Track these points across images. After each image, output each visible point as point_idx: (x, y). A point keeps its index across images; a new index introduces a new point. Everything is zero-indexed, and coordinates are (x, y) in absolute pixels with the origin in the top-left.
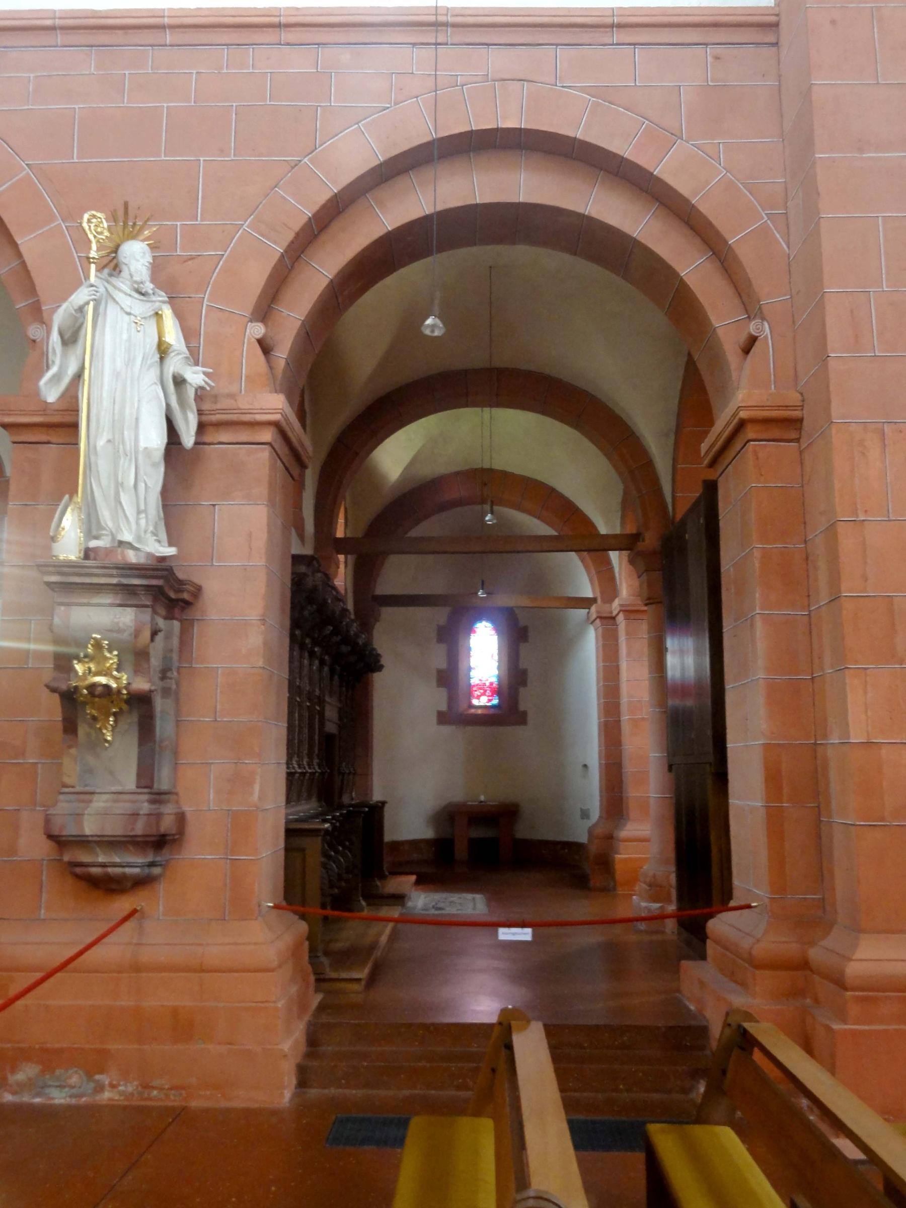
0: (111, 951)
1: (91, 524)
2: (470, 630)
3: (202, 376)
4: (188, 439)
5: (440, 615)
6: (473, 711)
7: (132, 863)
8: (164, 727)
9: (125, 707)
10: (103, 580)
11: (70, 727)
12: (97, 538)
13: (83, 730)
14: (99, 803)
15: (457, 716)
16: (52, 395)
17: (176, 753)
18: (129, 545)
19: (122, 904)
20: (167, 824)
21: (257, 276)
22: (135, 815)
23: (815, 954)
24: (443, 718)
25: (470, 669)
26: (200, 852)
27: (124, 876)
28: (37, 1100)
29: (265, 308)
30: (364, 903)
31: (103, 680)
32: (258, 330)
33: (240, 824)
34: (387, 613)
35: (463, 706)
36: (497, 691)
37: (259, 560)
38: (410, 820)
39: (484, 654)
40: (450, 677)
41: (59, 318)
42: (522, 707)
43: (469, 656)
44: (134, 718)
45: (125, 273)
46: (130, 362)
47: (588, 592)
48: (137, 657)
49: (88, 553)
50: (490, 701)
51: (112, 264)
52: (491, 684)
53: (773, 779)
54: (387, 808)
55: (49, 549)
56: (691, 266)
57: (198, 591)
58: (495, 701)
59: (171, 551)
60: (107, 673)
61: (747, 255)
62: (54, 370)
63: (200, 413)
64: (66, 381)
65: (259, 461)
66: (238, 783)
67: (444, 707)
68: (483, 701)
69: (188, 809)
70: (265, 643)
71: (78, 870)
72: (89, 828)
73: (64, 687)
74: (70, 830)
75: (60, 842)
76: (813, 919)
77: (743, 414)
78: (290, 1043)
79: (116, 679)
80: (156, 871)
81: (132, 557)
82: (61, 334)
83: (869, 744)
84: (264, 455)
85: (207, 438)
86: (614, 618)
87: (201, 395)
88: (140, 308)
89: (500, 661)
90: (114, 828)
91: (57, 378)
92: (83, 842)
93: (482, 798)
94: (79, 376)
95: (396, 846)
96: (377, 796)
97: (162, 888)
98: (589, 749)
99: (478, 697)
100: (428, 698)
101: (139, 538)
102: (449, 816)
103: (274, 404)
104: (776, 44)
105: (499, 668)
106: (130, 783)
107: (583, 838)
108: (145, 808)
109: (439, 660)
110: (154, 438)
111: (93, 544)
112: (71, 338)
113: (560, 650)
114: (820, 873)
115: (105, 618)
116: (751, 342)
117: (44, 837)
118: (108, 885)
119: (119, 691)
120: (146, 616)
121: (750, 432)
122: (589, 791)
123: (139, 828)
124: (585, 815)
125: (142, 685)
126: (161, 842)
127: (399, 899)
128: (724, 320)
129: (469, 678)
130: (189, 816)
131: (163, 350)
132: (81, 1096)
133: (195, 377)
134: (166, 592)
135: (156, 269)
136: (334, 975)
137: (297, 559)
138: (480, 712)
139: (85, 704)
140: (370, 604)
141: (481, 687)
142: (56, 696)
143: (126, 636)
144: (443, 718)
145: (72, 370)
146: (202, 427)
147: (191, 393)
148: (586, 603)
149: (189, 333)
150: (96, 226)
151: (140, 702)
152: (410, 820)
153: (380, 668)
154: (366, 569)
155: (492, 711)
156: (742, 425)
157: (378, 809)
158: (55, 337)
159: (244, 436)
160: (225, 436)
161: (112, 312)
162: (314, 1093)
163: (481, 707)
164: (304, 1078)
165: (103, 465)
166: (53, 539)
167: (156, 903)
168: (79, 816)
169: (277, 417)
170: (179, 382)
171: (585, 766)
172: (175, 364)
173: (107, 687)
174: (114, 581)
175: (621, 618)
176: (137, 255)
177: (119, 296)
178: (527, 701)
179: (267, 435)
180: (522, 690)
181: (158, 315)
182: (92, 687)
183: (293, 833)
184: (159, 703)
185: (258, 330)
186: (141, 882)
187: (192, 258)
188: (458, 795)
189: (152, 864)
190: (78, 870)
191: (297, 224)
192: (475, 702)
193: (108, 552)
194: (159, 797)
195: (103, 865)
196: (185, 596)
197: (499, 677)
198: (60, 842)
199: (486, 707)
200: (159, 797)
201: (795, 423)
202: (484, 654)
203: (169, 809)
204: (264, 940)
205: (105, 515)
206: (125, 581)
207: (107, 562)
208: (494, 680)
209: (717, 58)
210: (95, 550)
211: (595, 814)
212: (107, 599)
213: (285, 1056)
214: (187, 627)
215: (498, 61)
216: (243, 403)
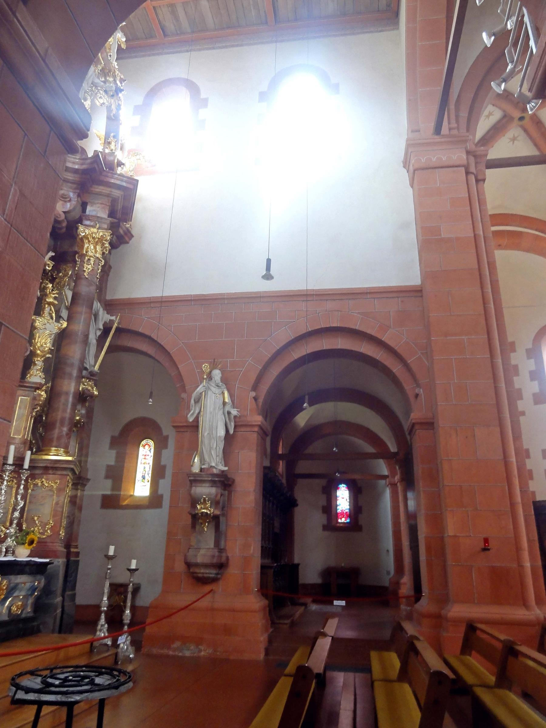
0: (205, 603)
1: (202, 460)
3: (236, 412)
4: (231, 431)
5: (323, 482)
6: (338, 525)
7: (211, 573)
8: (222, 527)
9: (211, 520)
10: (206, 479)
11: (194, 526)
12: (204, 464)
13: (198, 527)
14: (202, 552)
16: (191, 420)
17: (226, 537)
18: (214, 467)
19: (207, 588)
20: (223, 560)
21: (253, 377)
22: (213, 556)
23: (443, 612)
24: (326, 528)
25: (337, 506)
26: (233, 571)
27: (209, 578)
28: (180, 654)
29: (255, 388)
30: (289, 604)
31: (205, 511)
32: (253, 394)
33: (246, 560)
34: (300, 481)
35: (334, 523)
36: (349, 516)
37: (253, 470)
38: (310, 574)
39: (343, 499)
41: (194, 395)
42: (360, 523)
43: (336, 500)
44: (214, 523)
45: (213, 380)
46: (214, 409)
47: (386, 472)
48: (216, 503)
49: (201, 470)
50: (346, 520)
51: (210, 377)
52: (346, 513)
53: (429, 549)
54: (300, 567)
55: (190, 468)
56: (396, 369)
57: (234, 481)
58: (348, 520)
59: (226, 468)
60: (207, 509)
61: (414, 367)
62: (192, 412)
63: (235, 422)
64: (195, 415)
65: (253, 437)
66: (245, 546)
67: (325, 522)
68: (343, 520)
69: (230, 555)
70: (255, 499)
71: (195, 575)
72: (199, 560)
73: (194, 513)
74: (193, 561)
75: (189, 565)
76: (443, 600)
77: (413, 421)
78: (263, 638)
79: (210, 511)
80: (219, 576)
81: (215, 471)
82: (194, 400)
83: (455, 536)
84: (255, 435)
85: (237, 430)
86: (396, 484)
87: (235, 417)
88: (217, 391)
89: (350, 502)
90: (207, 560)
91: (193, 414)
92: (197, 565)
93: (343, 565)
94: (199, 413)
95: (305, 586)
96: (296, 561)
97: (221, 582)
98: (388, 543)
99: (341, 519)
100: (318, 519)
101: (217, 465)
102: (328, 573)
103: (258, 419)
104: (422, 296)
105: (350, 505)
106: (212, 545)
107: (387, 584)
108: (217, 554)
109: (323, 501)
110: (222, 433)
111: (203, 467)
112: (197, 401)
113: (377, 497)
114: (445, 584)
115: (205, 490)
116: (417, 396)
117: (183, 563)
118: (203, 581)
119: (210, 514)
120: (220, 491)
121: (417, 427)
122: (389, 562)
123: (215, 561)
124: (388, 573)
125: (217, 512)
126: (221, 566)
127: (305, 605)
128: (408, 386)
129: (337, 510)
130: (230, 558)
131: (224, 403)
132: (194, 653)
133: (234, 412)
134: (225, 482)
135: (223, 380)
136: (278, 622)
137: (265, 468)
138: (341, 525)
139: (199, 519)
140: (293, 477)
141: (342, 514)
142: (190, 516)
143: (213, 497)
144: (326, 528)
145: (197, 412)
146: (235, 427)
147: (232, 417)
148: (384, 477)
149: (231, 396)
150: (206, 367)
151: (216, 519)
152: (310, 574)
153: (297, 505)
154: (290, 466)
155: (347, 525)
156: (413, 425)
157: (296, 567)
158: (192, 401)
159: (248, 429)
160: (242, 429)
161: (210, 393)
162: (271, 657)
163: (342, 523)
164: (267, 652)
165: (206, 441)
166: (192, 466)
167: (219, 587)
168: (196, 556)
169: (260, 423)
170: (229, 413)
171: (388, 551)
172: (228, 408)
173: (207, 513)
174: (210, 479)
175: (398, 484)
176: (217, 374)
177: (212, 388)
178: (363, 520)
179: (256, 429)
180: (360, 515)
181: (223, 393)
182: (203, 512)
183: (263, 568)
184: (222, 519)
185: (253, 394)
186: (214, 580)
187: (232, 371)
188: (332, 563)
189: (217, 574)
190: (195, 575)
191: (267, 359)
192: (339, 521)
193: (208, 469)
194: (221, 551)
195: (203, 573)
196: (230, 483)
197: (350, 509)
198: (189, 565)
199: (344, 523)
200: (221, 551)
201: (433, 424)
202: (343, 499)
203: (224, 555)
204: (255, 602)
205: (206, 457)
206: (213, 479)
207: (209, 472)
208: (348, 511)
209: (402, 301)
210: (204, 468)
212: (207, 485)
213: (261, 642)
214: (230, 493)
215: (330, 305)
216: (249, 419)
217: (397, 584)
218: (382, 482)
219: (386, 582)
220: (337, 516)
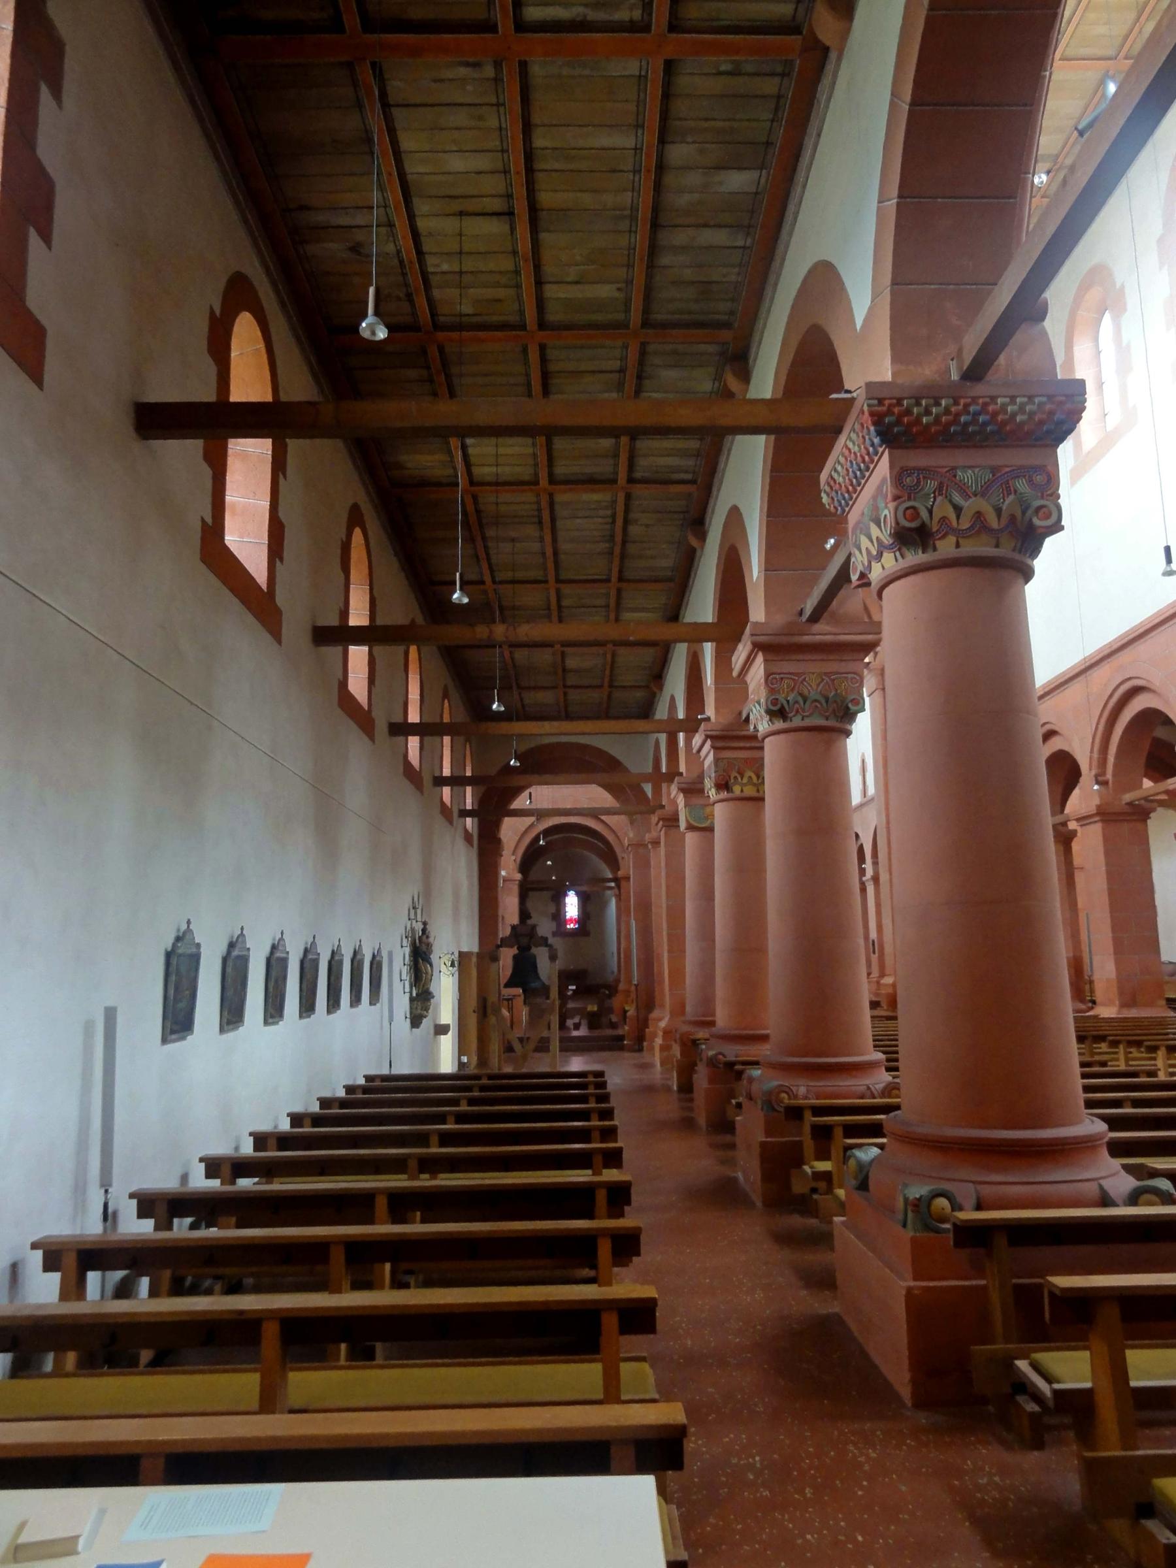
2: (566, 895)
15: (561, 932)
21: (513, 845)
34: (531, 894)
36: (578, 921)
39: (572, 906)
40: (558, 915)
56: (611, 838)
65: (515, 889)
103: (519, 876)
109: (552, 909)
113: (604, 905)
141: (571, 920)
148: (611, 888)
202: (572, 906)
211: (616, 970)
217: (618, 981)
218: (609, 892)
219: (610, 979)
220: (566, 922)
